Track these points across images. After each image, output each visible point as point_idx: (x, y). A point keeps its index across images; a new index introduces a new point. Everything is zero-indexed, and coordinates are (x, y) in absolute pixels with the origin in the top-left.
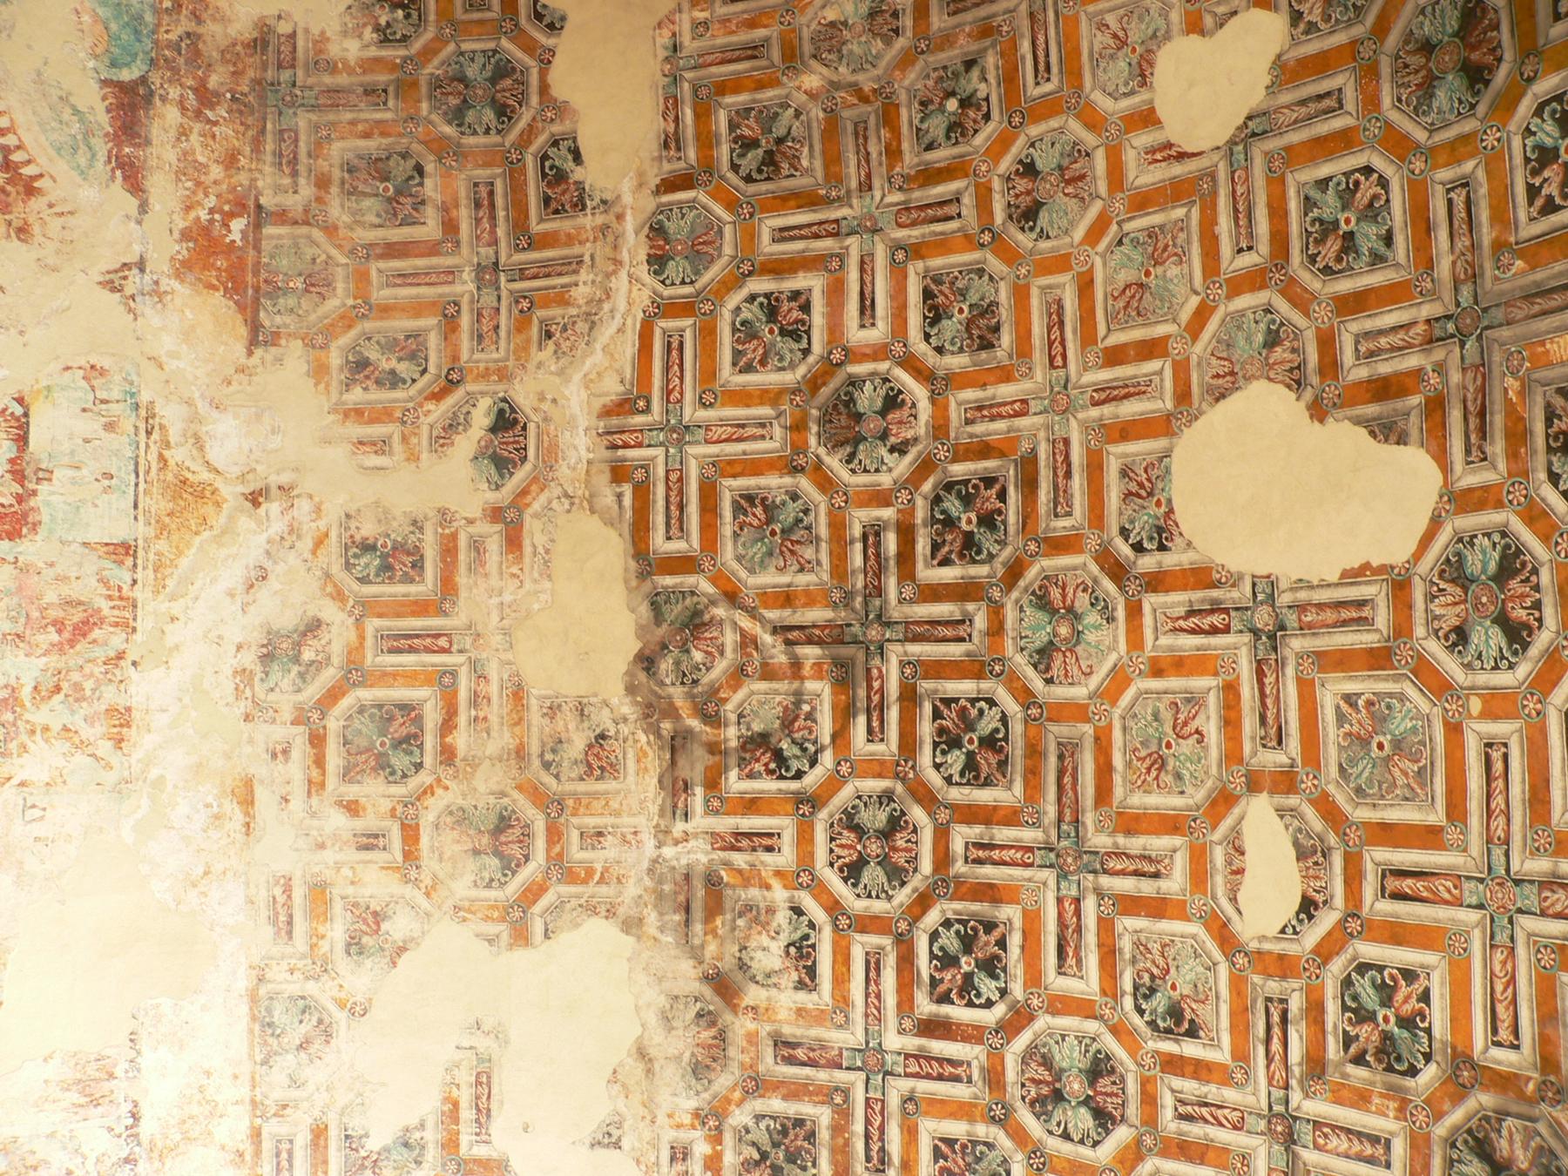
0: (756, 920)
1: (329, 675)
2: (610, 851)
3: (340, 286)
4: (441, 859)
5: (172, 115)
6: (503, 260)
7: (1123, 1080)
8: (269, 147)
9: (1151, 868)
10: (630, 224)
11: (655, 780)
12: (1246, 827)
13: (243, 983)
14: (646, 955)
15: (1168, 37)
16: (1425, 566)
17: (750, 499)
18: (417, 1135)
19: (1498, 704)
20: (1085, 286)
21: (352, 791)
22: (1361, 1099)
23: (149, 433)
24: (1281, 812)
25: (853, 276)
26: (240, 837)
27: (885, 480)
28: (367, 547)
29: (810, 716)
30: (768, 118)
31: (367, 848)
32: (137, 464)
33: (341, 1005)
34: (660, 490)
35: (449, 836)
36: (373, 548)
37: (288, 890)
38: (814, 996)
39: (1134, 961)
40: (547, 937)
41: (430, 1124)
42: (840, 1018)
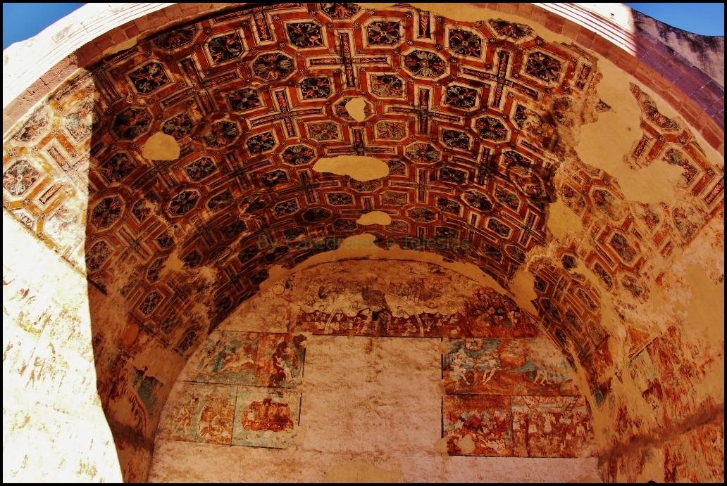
0: (534, 130)
1: (628, 274)
2: (574, 173)
3: (589, 320)
4: (621, 213)
5: (599, 379)
6: (556, 287)
7: (406, 65)
8: (590, 352)
9: (394, 109)
10: (528, 265)
11: (556, 176)
12: (364, 117)
13: (688, 250)
14: (572, 143)
15: (387, 226)
16: (315, 158)
17: (512, 207)
18: (667, 158)
19: (294, 142)
20: (412, 200)
21: (635, 249)
22: (321, 71)
23: (632, 355)
24: (353, 119)
25: (477, 223)
26: (666, 275)
27: (476, 190)
28: (607, 282)
29: (506, 161)
30: (491, 255)
31: (639, 235)
32: (638, 355)
33: (668, 212)
34: (535, 224)
35: (617, 214)
36: (605, 279)
37: (662, 252)
38: (519, 103)
39: (402, 92)
40: (599, 170)
41: (661, 157)
42: (511, 95)
